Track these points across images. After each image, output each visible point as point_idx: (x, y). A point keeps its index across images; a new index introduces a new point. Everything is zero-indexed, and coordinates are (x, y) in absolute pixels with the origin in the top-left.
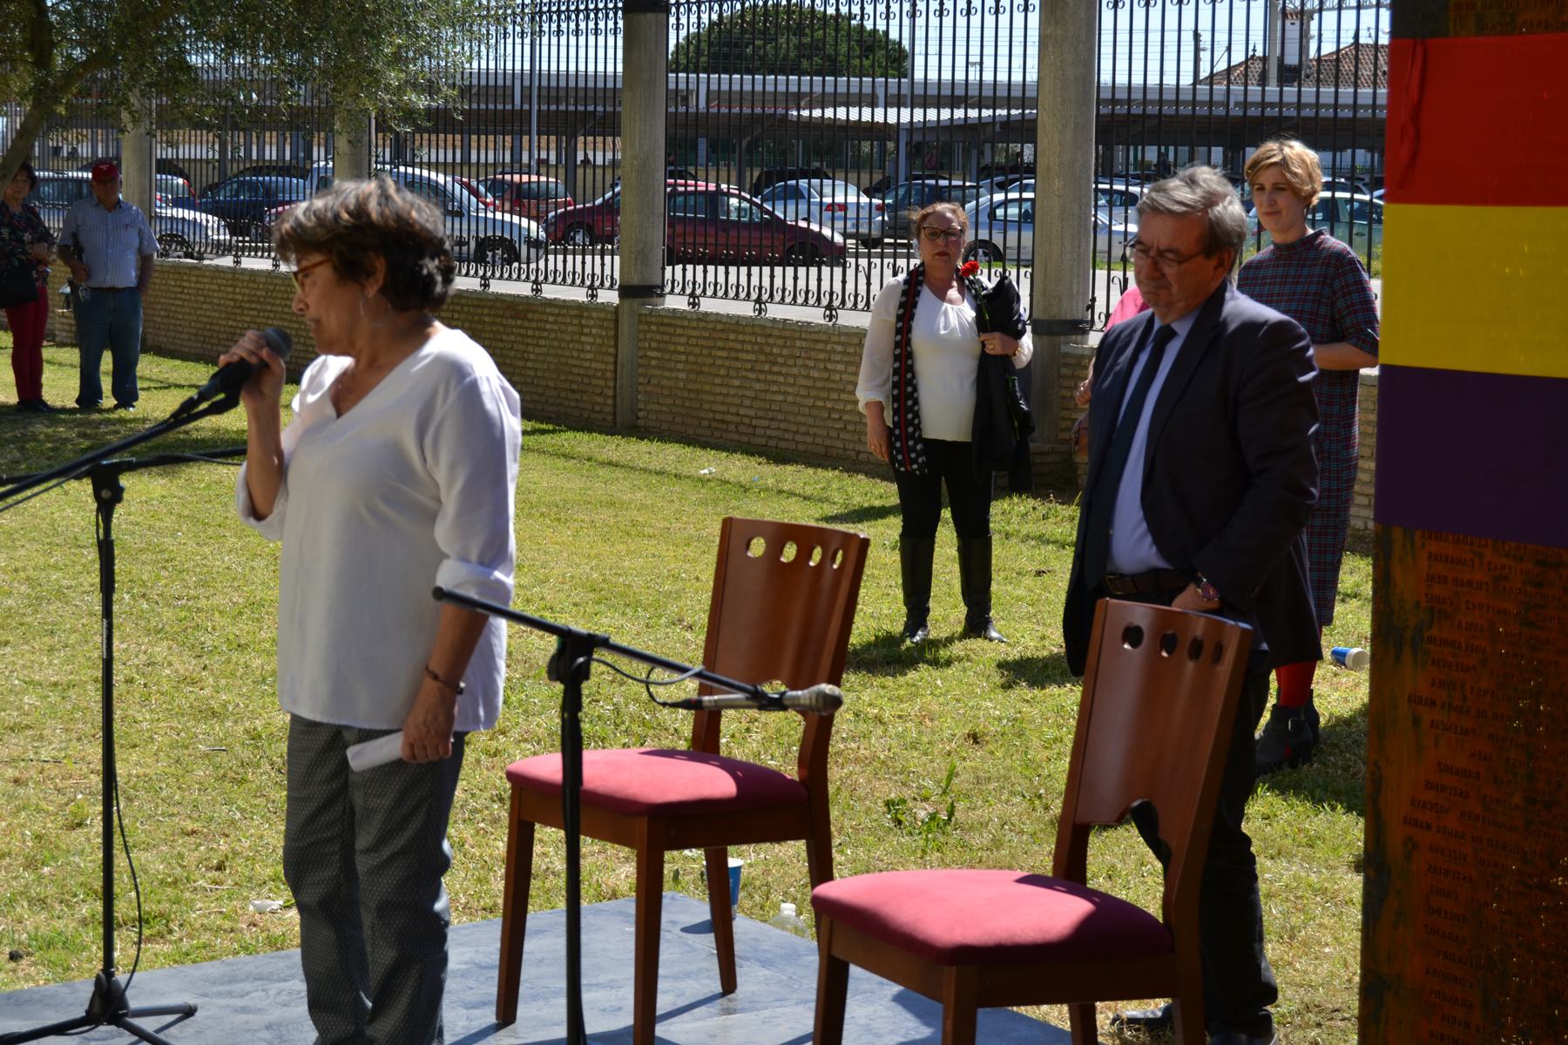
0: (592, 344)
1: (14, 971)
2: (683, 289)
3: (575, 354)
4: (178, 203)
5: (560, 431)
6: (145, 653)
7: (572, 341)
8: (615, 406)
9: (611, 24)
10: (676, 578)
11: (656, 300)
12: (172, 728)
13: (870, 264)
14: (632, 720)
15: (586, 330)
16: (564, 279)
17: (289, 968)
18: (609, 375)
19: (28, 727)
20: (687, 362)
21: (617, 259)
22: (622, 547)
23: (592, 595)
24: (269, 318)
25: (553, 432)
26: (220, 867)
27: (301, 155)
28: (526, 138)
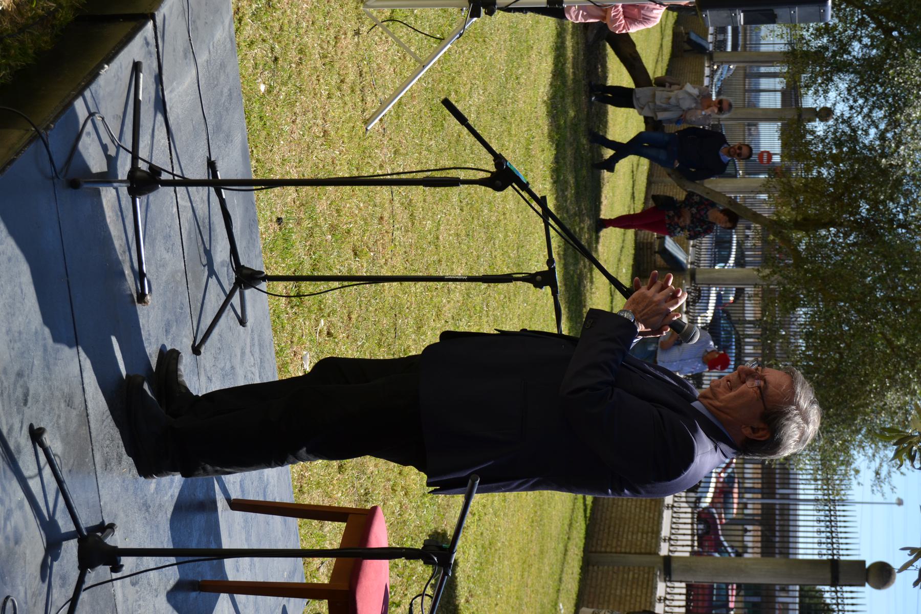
0: (637, 539)
1: (271, 221)
2: (669, 594)
3: (631, 529)
4: (719, 297)
5: (586, 521)
6: (456, 288)
7: (638, 527)
8: (601, 552)
9: (824, 552)
10: (497, 592)
11: (663, 577)
12: (411, 304)
14: (413, 569)
15: (645, 536)
16: (674, 523)
18: (619, 549)
19: (413, 224)
21: (687, 554)
22: (516, 559)
23: (487, 543)
25: (585, 517)
26: (329, 334)
28: (760, 496)
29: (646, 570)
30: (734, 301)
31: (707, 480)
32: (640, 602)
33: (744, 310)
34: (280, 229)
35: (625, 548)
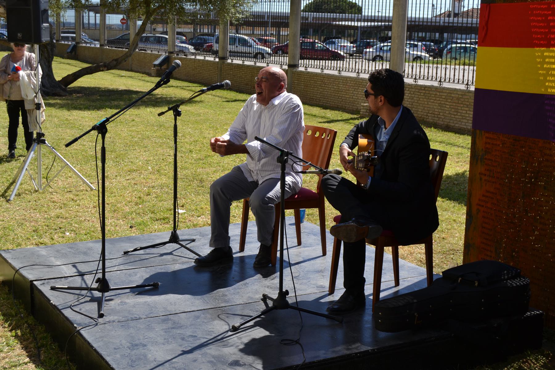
2: (304, 66)
11: (296, 68)
13: (349, 60)
16: (274, 63)
17: (197, 232)
20: (304, 84)
21: (287, 58)
27: (213, 31)
28: (268, 28)
29: (293, 75)
30: (185, 36)
31: (261, 50)
32: (307, 78)
33: (189, 32)
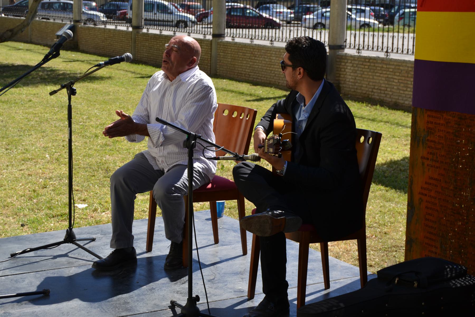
2: (230, 35)
11: (222, 38)
18: (209, 60)
20: (231, 56)
24: (114, 42)
29: (219, 46)
32: (234, 49)
34: (27, 225)
35: (208, 56)
